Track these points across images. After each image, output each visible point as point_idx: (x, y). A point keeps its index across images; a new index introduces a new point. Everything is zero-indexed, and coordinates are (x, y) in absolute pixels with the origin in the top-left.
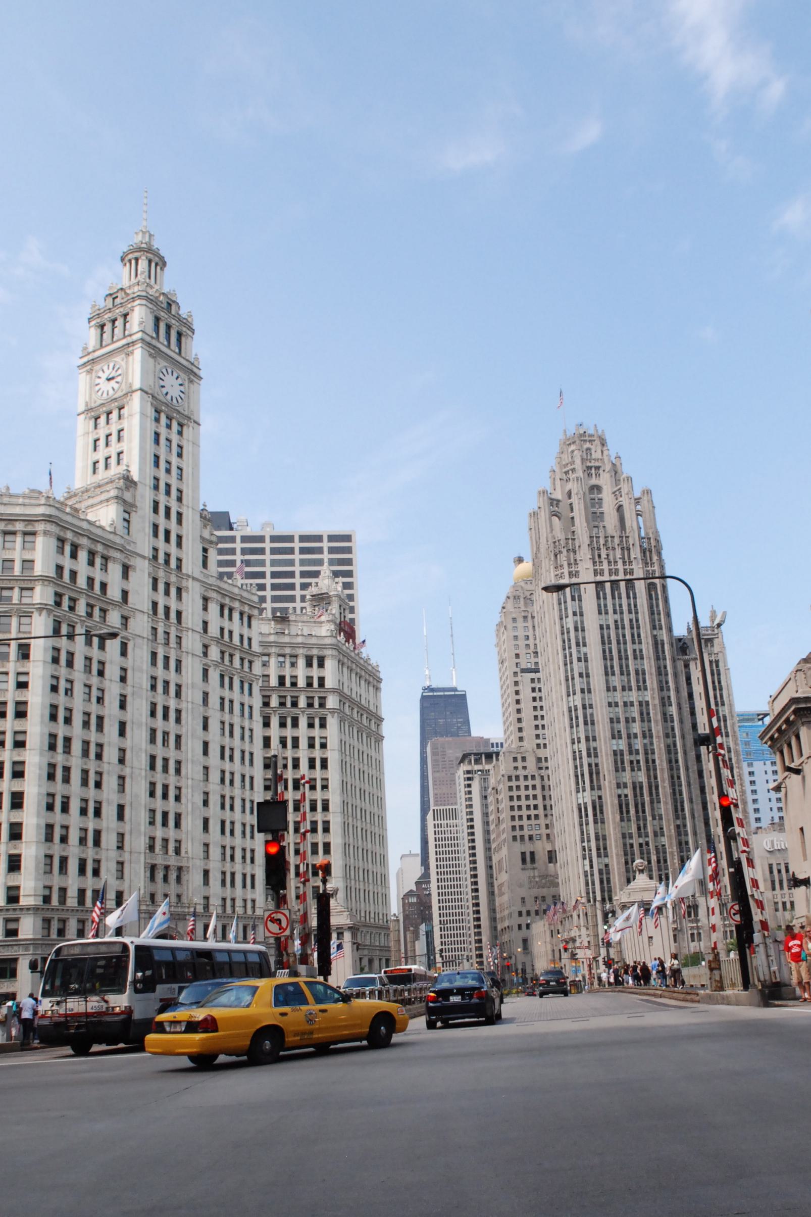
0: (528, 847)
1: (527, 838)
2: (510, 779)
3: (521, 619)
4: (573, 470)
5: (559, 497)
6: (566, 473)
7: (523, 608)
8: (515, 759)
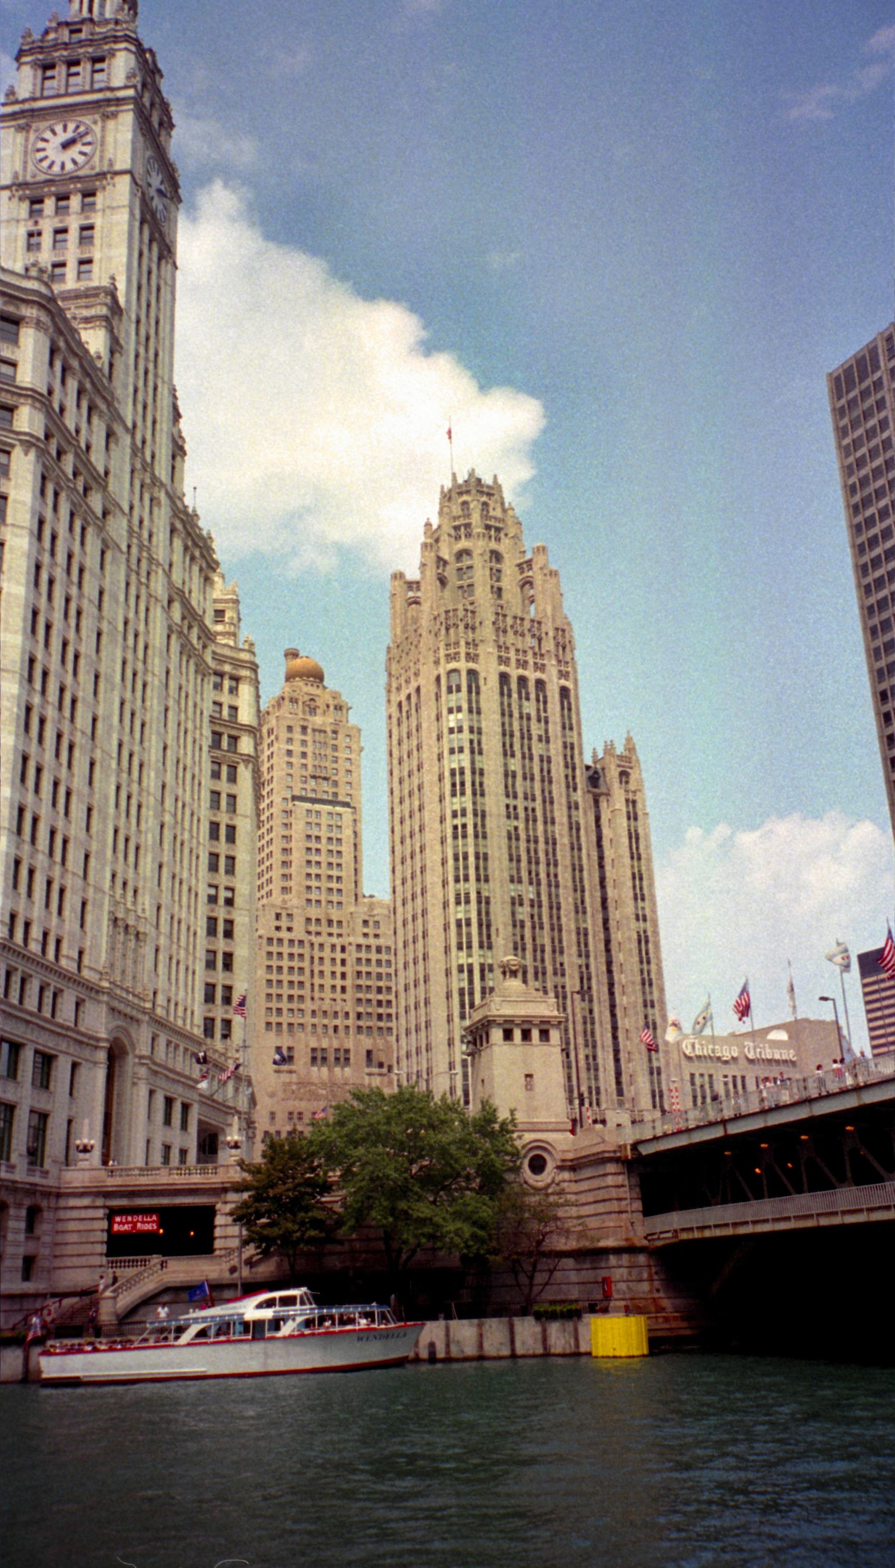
0: (285, 1042)
1: (285, 1026)
2: (270, 940)
3: (299, 730)
4: (468, 526)
6: (456, 528)
7: (301, 716)
8: (278, 916)
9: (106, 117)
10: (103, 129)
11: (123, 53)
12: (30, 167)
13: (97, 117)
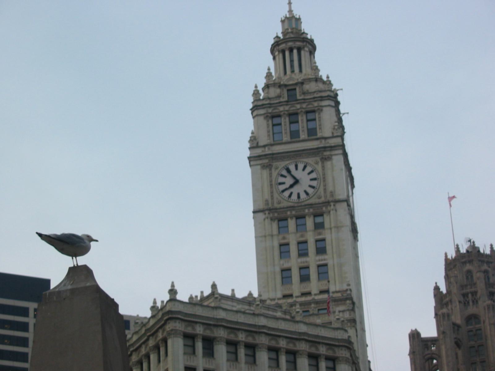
5: (458, 322)
9: (325, 159)
10: (323, 167)
11: (328, 108)
12: (276, 195)
13: (318, 159)
